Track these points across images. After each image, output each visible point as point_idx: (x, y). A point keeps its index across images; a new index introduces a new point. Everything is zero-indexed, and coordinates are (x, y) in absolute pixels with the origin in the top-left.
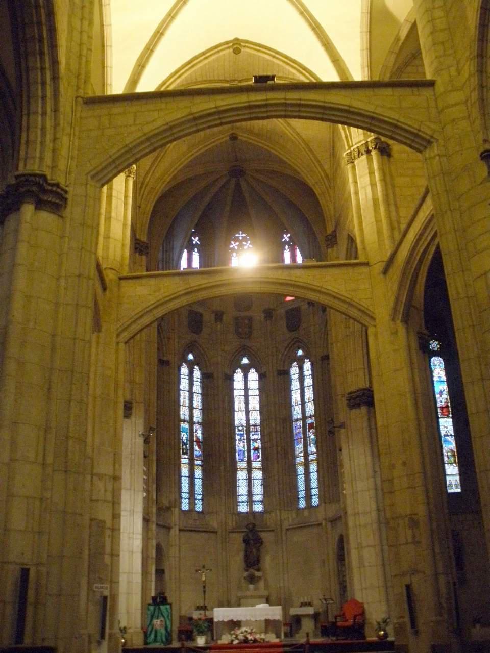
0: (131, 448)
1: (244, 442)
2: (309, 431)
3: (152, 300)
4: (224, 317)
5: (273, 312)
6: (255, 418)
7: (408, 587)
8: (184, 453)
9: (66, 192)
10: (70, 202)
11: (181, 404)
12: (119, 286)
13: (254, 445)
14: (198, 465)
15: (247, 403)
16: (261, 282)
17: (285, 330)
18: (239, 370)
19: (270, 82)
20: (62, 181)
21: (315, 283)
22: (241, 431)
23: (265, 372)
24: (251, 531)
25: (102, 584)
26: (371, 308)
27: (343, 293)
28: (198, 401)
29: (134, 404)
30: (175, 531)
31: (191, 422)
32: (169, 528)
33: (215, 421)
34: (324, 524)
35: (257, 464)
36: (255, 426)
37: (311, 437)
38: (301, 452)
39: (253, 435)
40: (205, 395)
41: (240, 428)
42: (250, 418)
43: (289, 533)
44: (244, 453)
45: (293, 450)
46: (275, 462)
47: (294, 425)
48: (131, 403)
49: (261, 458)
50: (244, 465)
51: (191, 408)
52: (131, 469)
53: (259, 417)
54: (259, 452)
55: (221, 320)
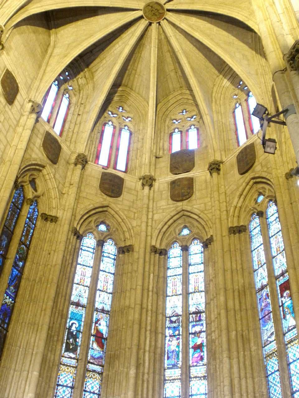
1: (178, 339)
2: (282, 296)
4: (156, 185)
5: (221, 165)
6: (198, 301)
8: (68, 350)
11: (76, 281)
13: (194, 341)
14: (94, 371)
15: (186, 282)
17: (238, 176)
18: (177, 245)
22: (175, 322)
23: (212, 236)
28: (106, 281)
31: (91, 307)
33: (129, 307)
35: (199, 370)
36: (198, 313)
37: (286, 305)
38: (272, 334)
39: (194, 326)
40: (119, 275)
41: (174, 319)
42: (191, 302)
44: (178, 355)
45: (258, 335)
46: (225, 355)
47: (259, 297)
49: (205, 361)
50: (176, 373)
51: (93, 289)
53: (203, 300)
54: (202, 351)
55: (151, 186)
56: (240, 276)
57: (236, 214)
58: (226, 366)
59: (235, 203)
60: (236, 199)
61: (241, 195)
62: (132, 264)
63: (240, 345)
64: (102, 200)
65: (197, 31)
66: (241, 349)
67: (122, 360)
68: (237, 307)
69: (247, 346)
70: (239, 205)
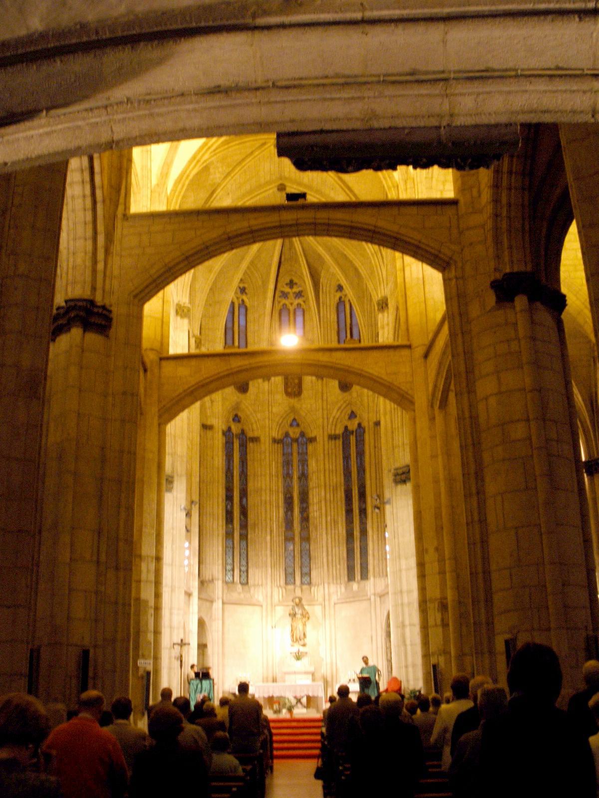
0: (173, 524)
3: (193, 381)
7: (434, 667)
9: (110, 312)
10: (114, 321)
12: (160, 368)
16: (302, 364)
19: (301, 202)
20: (107, 302)
21: (356, 366)
24: (297, 605)
25: (146, 659)
26: (410, 392)
27: (383, 376)
29: (176, 478)
30: (218, 605)
32: (212, 602)
33: (261, 489)
34: (372, 598)
43: (337, 606)
46: (324, 533)
48: (172, 477)
52: (173, 544)
56: (334, 477)
57: (334, 423)
58: (325, 539)
59: (334, 414)
60: (335, 411)
61: (340, 408)
62: (260, 454)
63: (333, 525)
64: (236, 398)
65: (320, 245)
66: (333, 528)
67: (260, 526)
68: (332, 499)
69: (336, 526)
70: (337, 417)
